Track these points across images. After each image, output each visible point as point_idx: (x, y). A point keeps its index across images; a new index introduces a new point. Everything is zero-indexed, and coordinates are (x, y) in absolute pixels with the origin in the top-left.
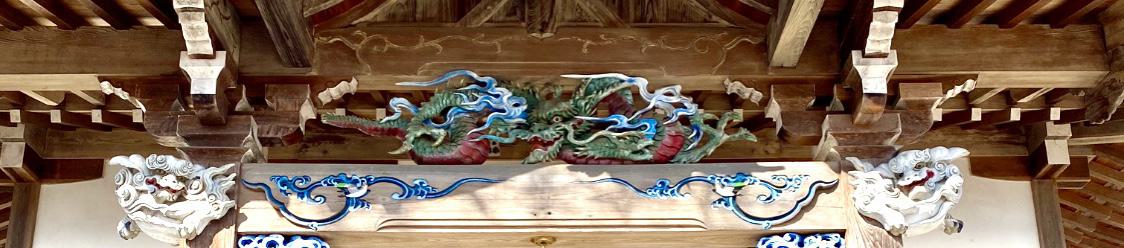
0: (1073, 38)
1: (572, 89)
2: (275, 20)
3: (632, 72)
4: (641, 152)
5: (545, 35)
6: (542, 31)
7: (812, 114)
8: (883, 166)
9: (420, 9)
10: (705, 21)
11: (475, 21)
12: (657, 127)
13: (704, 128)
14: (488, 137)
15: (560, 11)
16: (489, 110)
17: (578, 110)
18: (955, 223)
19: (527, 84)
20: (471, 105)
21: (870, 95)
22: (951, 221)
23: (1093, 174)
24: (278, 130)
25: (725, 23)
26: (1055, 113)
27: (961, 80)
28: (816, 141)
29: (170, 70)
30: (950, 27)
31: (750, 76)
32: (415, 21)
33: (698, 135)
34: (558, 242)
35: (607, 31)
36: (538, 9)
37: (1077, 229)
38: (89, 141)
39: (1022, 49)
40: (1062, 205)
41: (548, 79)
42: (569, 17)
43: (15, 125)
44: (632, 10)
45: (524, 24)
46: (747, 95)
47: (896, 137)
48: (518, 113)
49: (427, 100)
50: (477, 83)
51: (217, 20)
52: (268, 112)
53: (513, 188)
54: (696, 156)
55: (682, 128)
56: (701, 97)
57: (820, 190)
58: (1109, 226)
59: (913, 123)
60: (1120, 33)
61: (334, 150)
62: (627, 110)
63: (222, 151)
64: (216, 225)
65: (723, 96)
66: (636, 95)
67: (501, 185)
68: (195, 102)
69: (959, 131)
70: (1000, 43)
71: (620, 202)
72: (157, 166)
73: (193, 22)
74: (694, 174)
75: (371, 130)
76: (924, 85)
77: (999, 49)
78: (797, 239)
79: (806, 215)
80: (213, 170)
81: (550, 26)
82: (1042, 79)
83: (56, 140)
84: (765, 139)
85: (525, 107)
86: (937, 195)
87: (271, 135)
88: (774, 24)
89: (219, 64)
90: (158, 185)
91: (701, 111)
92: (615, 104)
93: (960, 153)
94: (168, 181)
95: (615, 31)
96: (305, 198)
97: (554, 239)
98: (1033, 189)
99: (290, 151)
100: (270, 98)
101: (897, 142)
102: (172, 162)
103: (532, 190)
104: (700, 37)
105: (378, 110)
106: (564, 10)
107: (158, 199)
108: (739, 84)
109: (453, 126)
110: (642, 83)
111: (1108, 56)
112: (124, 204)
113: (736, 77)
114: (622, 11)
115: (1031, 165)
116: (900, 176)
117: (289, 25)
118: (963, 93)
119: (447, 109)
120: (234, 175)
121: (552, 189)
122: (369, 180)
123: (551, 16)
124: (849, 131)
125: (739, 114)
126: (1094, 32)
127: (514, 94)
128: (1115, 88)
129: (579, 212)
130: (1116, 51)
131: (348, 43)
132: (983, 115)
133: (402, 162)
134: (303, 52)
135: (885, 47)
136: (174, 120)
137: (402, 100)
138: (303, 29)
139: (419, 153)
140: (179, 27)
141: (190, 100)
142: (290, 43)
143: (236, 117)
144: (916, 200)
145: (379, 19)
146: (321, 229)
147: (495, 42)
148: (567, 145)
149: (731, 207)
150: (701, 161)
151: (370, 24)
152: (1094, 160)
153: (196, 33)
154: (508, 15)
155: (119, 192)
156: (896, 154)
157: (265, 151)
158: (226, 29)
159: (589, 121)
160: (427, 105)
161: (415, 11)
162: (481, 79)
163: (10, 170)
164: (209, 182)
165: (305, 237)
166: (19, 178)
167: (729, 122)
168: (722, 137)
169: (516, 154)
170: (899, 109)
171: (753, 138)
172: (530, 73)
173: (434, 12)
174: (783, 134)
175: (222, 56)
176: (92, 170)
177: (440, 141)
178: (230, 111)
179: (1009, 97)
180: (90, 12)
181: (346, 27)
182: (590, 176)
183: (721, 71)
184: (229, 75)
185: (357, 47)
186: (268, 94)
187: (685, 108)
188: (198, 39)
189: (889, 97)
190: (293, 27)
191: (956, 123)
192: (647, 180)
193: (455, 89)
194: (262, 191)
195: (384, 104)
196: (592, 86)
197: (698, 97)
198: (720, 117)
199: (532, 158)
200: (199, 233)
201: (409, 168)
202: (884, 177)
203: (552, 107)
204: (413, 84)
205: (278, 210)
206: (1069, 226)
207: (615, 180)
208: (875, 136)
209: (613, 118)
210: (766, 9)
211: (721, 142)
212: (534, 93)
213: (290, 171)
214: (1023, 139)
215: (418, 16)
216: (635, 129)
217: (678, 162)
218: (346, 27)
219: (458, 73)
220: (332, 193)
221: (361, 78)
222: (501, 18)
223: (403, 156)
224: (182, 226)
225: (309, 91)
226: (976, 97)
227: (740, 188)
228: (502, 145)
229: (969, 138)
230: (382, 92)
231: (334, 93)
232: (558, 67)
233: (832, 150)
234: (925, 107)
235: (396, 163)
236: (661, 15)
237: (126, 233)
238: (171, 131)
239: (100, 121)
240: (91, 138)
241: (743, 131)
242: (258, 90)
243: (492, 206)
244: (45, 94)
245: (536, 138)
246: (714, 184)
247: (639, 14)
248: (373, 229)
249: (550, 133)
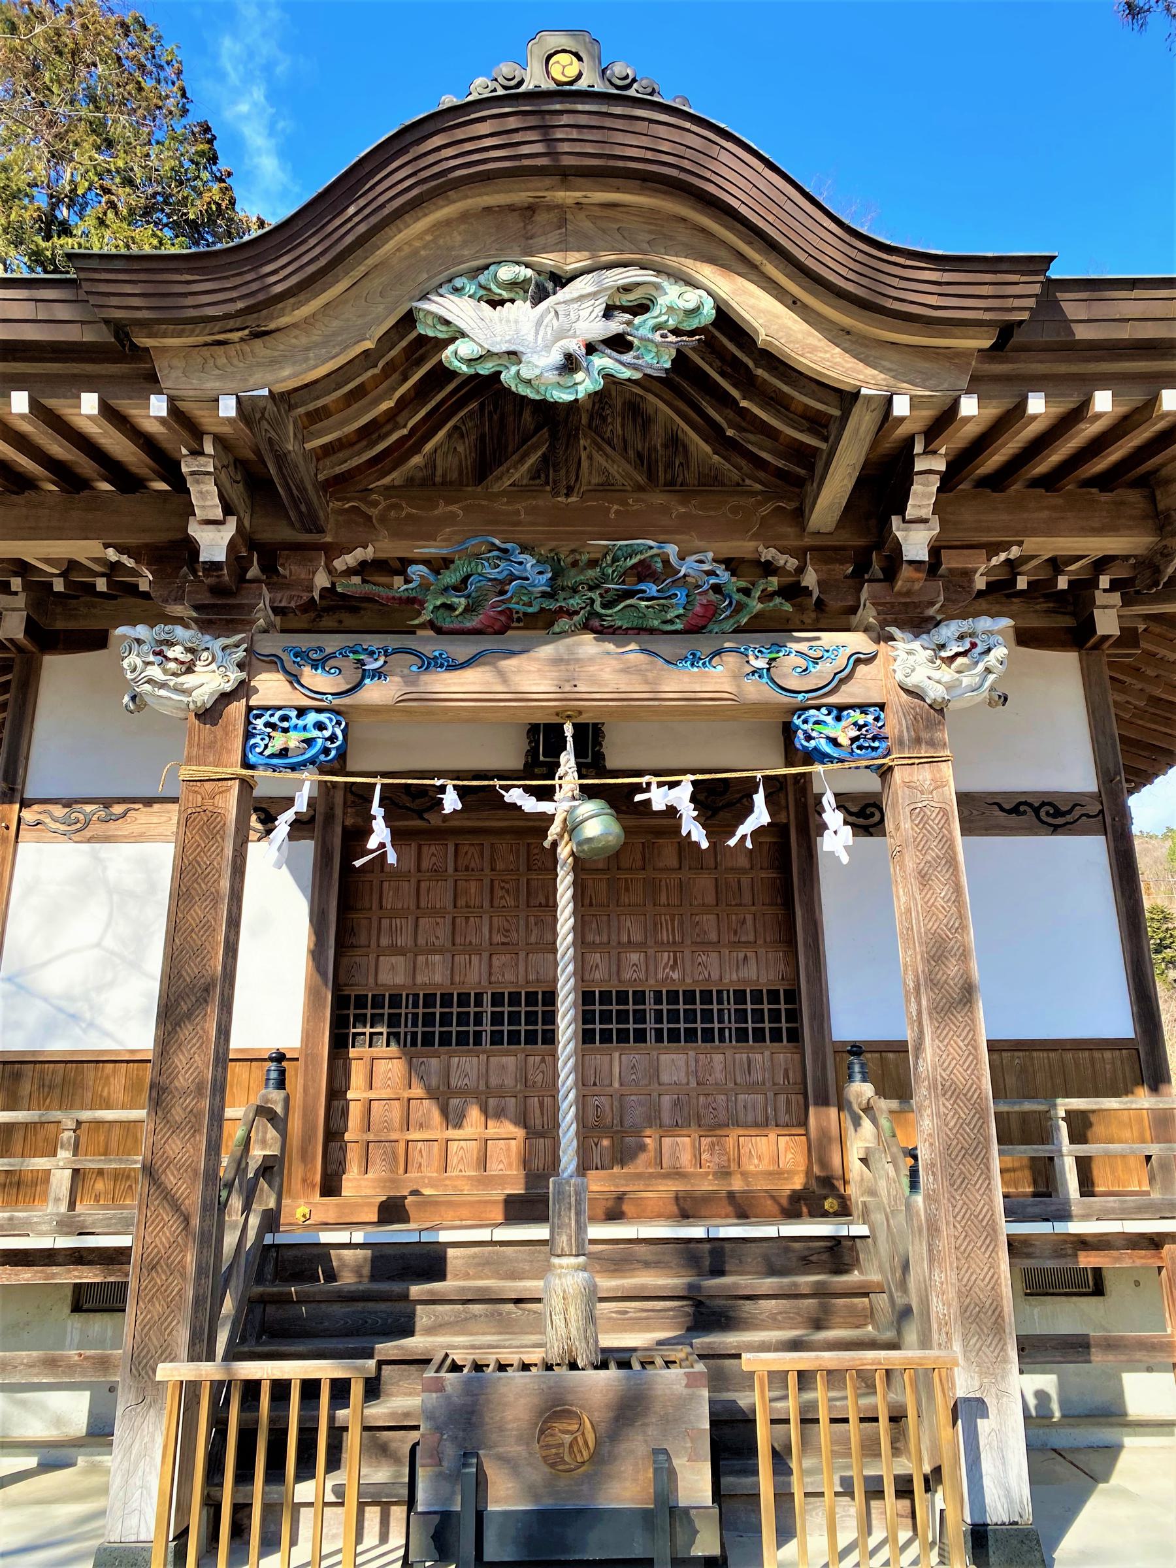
0: (1123, 503)
1: (599, 556)
2: (288, 484)
3: (662, 537)
4: (671, 622)
5: (570, 500)
6: (567, 495)
7: (850, 582)
8: (924, 636)
9: (439, 472)
10: (738, 485)
11: (497, 485)
12: (687, 596)
13: (737, 597)
14: (512, 606)
15: (586, 475)
16: (512, 578)
17: (605, 578)
18: (1000, 697)
19: (551, 551)
20: (493, 573)
21: (911, 562)
22: (995, 695)
23: (1144, 645)
24: (291, 598)
25: (758, 487)
26: (1104, 581)
27: (1006, 547)
28: (854, 610)
29: (180, 536)
30: (994, 491)
31: (786, 543)
32: (434, 484)
33: (730, 604)
34: (584, 716)
35: (635, 495)
36: (563, 472)
37: (1127, 702)
38: (93, 611)
39: (1069, 514)
40: (1111, 678)
41: (573, 546)
42: (595, 480)
43: (16, 593)
44: (661, 474)
45: (548, 488)
46: (782, 562)
47: (938, 606)
48: (542, 582)
49: (447, 568)
50: (499, 549)
51: (227, 484)
52: (281, 580)
53: (538, 659)
54: (728, 626)
55: (713, 597)
56: (733, 565)
57: (858, 661)
58: (1161, 699)
59: (956, 591)
60: (1175, 498)
61: (349, 620)
62: (655, 578)
63: (232, 621)
64: (225, 698)
65: (757, 563)
66: (666, 562)
67: (525, 656)
68: (204, 570)
69: (1004, 600)
70: (1047, 508)
71: (649, 674)
72: (164, 636)
73: (202, 486)
74: (727, 645)
75: (388, 599)
76: (966, 552)
77: (1045, 514)
78: (835, 712)
79: (843, 688)
80: (223, 641)
81: (576, 490)
82: (1090, 545)
83: (59, 610)
84: (801, 609)
85: (550, 575)
86: (981, 667)
87: (283, 604)
88: (811, 488)
89: (228, 531)
90: (165, 657)
91: (734, 579)
92: (644, 571)
93: (1006, 623)
94: (176, 652)
95: (643, 496)
96: (319, 671)
97: (580, 713)
98: (1081, 661)
99: (303, 621)
100: (282, 565)
101: (939, 611)
102: (179, 632)
103: (557, 661)
104: (735, 501)
105: (396, 578)
106: (590, 473)
107: (165, 671)
108: (773, 550)
109: (474, 595)
110: (672, 550)
111: (1160, 521)
112: (129, 676)
113: (772, 543)
114: (651, 475)
115: (1077, 635)
116: (942, 647)
117: (302, 489)
118: (1008, 561)
119: (468, 576)
120: (244, 646)
121: (578, 660)
122: (386, 651)
123: (577, 480)
124: (888, 599)
125: (774, 582)
126: (1145, 497)
127: (538, 562)
128: (1166, 555)
129: (606, 685)
130: (1168, 517)
131: (363, 507)
132: (1029, 583)
133: (420, 633)
134: (318, 518)
135: (926, 512)
136: (182, 588)
137: (421, 567)
138: (317, 493)
139: (438, 623)
140: (188, 491)
141: (200, 567)
142: (303, 508)
143: (246, 585)
144: (959, 672)
145: (397, 483)
146: (335, 702)
147: (518, 506)
148: (593, 614)
149: (765, 680)
150: (734, 631)
151: (387, 488)
152: (1145, 630)
153: (205, 497)
154: (532, 478)
155: (125, 664)
156: (938, 624)
157: (277, 620)
158: (236, 494)
159: (617, 590)
160: (447, 572)
161: (434, 474)
162: (503, 546)
163: (11, 640)
164: (219, 654)
165: (319, 710)
166: (20, 649)
167: (763, 591)
168: (756, 606)
169: (540, 624)
170: (942, 576)
171: (788, 607)
172: (555, 540)
173: (455, 475)
174: (820, 604)
175: (232, 522)
176: (97, 641)
177: (460, 610)
178: (241, 579)
179: (1056, 564)
180: (95, 476)
181: (362, 491)
182: (618, 646)
183: (756, 537)
184: (240, 541)
185: (374, 512)
186: (281, 561)
187: (717, 575)
188: (208, 503)
189: (930, 564)
190: (306, 490)
191: (999, 593)
192: (678, 651)
193: (477, 556)
194: (274, 662)
195: (402, 572)
196: (619, 553)
197: (732, 564)
198: (753, 585)
199: (556, 629)
200: (208, 706)
201: (427, 640)
202: (925, 648)
203: (578, 575)
204: (432, 550)
205: (291, 683)
206: (1118, 699)
207: (643, 651)
208: (916, 605)
209: (642, 587)
210: (802, 472)
211: (755, 612)
212: (559, 560)
213: (304, 641)
214: (1070, 608)
215: (438, 479)
216: (665, 598)
217: (710, 632)
218: (362, 491)
219: (480, 539)
220: (347, 664)
221: (378, 545)
222: (524, 482)
223: (422, 626)
224: (190, 699)
225: (323, 558)
226: (1022, 565)
227: (774, 659)
228: (525, 614)
229: (1014, 608)
230: (401, 560)
231: (349, 560)
232: (583, 533)
233: (871, 620)
234: (968, 574)
235: (414, 633)
236: (691, 478)
237: (132, 706)
238: (179, 600)
239: (105, 589)
240: (95, 607)
241: (778, 600)
242: (270, 555)
243: (516, 679)
244: (47, 561)
245: (561, 607)
246: (747, 656)
247: (669, 477)
248: (391, 703)
249: (575, 602)
